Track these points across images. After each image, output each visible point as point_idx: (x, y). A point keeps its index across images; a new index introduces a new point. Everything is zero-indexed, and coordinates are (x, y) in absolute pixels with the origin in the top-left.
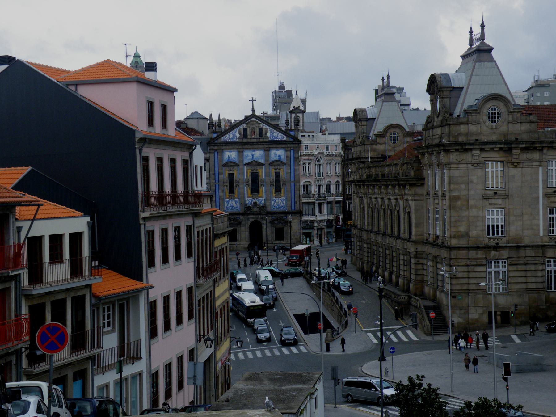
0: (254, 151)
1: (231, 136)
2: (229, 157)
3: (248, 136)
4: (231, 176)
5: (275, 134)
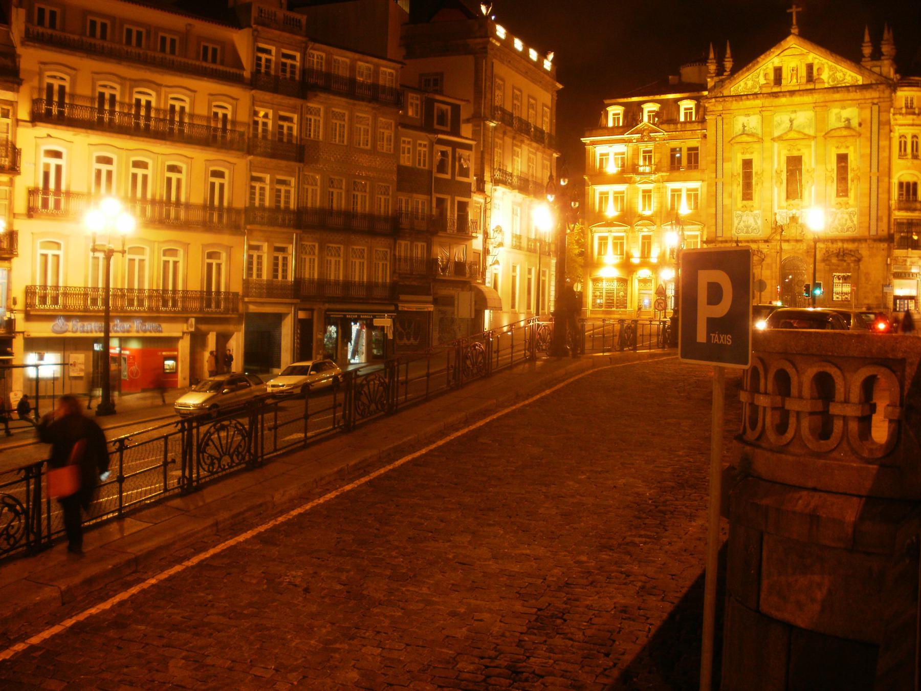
0: (795, 111)
1: (750, 83)
2: (744, 127)
3: (784, 82)
4: (747, 164)
5: (839, 75)
